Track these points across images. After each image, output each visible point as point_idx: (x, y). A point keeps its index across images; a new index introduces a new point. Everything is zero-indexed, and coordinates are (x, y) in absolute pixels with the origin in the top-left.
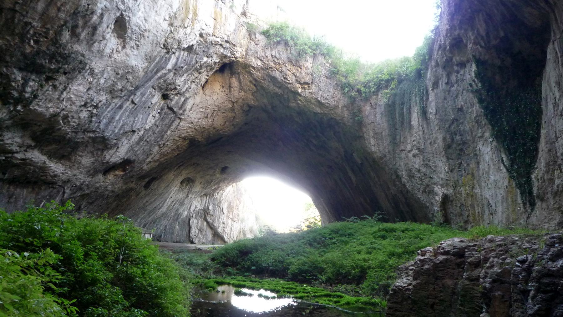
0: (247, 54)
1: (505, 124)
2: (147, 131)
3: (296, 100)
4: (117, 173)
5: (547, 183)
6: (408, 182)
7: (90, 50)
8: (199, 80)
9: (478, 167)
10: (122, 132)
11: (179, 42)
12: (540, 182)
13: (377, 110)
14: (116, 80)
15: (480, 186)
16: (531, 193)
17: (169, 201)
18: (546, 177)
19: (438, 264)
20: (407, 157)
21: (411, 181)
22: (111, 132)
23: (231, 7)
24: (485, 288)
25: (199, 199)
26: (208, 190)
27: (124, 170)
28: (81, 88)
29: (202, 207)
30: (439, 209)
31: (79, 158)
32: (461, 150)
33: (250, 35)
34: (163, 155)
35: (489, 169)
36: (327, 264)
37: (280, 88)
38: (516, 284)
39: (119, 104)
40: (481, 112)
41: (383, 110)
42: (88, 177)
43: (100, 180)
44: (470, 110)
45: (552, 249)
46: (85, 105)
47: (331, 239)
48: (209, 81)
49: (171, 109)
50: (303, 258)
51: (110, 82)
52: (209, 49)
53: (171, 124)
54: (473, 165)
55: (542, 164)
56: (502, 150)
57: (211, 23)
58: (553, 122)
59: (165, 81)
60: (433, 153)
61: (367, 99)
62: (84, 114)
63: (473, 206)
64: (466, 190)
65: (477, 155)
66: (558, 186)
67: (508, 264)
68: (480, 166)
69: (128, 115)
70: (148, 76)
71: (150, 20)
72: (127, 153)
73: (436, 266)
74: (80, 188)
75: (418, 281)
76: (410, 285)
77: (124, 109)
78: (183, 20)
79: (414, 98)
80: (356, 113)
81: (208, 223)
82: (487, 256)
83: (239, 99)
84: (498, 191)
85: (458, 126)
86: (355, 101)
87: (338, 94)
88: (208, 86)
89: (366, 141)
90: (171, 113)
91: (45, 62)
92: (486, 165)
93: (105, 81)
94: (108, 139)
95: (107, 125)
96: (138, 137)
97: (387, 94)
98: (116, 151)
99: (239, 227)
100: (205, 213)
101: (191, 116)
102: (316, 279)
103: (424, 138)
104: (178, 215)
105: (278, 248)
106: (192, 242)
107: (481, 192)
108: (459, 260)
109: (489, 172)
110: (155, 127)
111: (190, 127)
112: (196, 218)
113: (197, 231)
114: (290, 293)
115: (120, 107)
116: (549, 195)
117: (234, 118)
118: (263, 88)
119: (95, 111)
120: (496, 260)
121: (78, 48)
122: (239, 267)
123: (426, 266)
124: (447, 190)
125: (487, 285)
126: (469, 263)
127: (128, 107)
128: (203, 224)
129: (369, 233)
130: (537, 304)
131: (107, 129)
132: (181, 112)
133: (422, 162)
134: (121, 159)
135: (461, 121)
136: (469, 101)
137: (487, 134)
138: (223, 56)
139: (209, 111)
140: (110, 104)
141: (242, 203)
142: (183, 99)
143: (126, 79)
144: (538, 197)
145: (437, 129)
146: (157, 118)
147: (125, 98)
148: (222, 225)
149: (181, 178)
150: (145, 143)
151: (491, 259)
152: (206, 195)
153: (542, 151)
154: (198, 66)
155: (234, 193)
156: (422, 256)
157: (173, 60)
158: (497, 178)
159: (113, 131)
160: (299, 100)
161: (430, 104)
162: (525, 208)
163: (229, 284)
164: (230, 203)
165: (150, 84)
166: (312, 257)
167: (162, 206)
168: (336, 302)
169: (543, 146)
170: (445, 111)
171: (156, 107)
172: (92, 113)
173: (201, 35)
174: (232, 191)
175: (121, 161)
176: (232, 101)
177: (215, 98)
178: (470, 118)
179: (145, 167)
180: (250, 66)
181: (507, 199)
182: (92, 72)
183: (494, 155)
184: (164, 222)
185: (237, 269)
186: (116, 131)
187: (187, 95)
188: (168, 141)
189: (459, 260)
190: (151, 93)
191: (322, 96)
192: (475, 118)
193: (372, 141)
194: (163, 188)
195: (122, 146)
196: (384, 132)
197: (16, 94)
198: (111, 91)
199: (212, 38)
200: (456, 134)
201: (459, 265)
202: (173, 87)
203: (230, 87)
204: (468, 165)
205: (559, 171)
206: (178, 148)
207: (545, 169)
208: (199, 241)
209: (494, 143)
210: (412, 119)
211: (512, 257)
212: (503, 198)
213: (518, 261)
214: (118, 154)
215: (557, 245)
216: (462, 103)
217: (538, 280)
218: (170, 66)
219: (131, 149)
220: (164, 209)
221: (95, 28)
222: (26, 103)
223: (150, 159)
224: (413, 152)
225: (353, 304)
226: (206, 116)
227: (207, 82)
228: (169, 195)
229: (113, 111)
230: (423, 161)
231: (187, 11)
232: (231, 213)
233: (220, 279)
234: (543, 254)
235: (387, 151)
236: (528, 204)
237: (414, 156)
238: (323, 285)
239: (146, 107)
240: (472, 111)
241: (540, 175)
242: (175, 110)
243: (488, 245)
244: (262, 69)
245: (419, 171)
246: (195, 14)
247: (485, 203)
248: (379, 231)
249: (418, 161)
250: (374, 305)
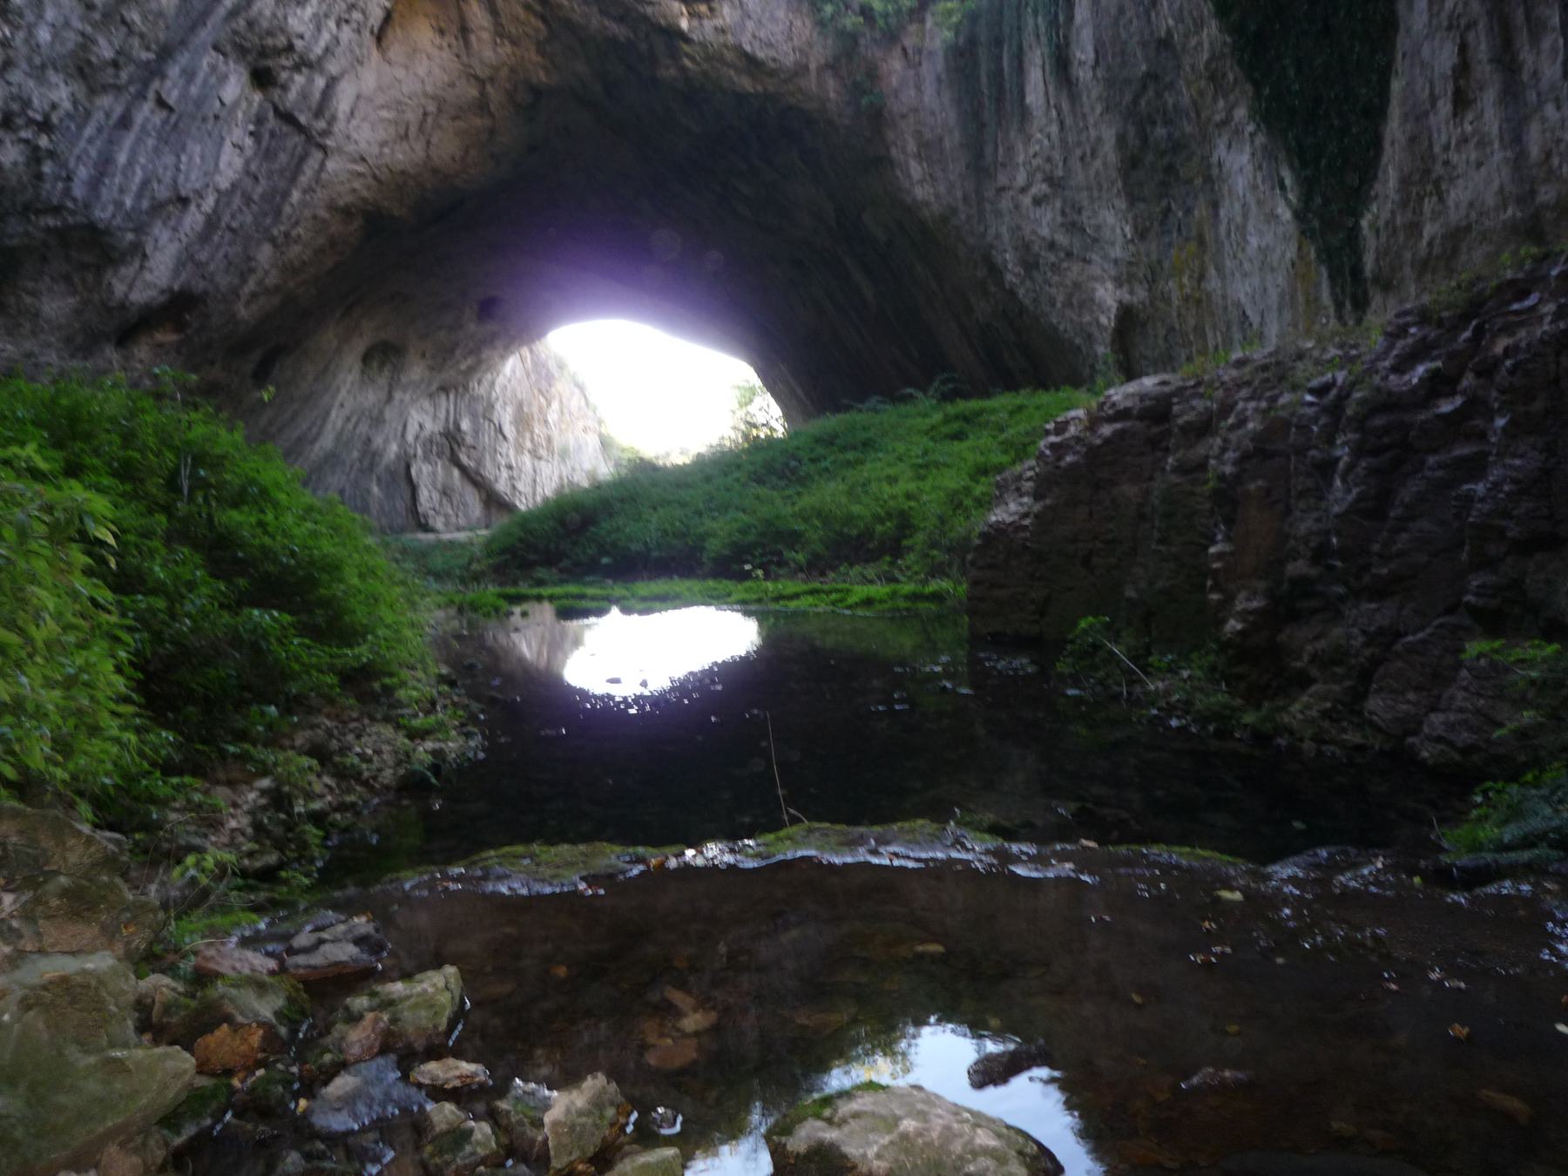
1: (1291, 72)
2: (224, 196)
3: (675, 55)
4: (160, 337)
5: (1401, 239)
6: (1022, 282)
8: (364, 13)
9: (1216, 215)
10: (145, 204)
12: (1383, 238)
13: (926, 68)
14: (89, 29)
15: (1220, 269)
16: (1357, 272)
17: (336, 418)
18: (1399, 221)
19: (1099, 447)
20: (1017, 207)
21: (1032, 280)
22: (111, 208)
24: (1222, 478)
25: (426, 404)
26: (449, 375)
27: (180, 327)
30: (1109, 350)
31: (28, 300)
32: (1170, 169)
34: (290, 270)
35: (1245, 216)
36: (806, 520)
37: (621, 19)
38: (1301, 451)
39: (118, 110)
40: (1225, 43)
41: (940, 64)
42: (73, 356)
43: (110, 362)
44: (1193, 42)
45: (1400, 343)
47: (813, 461)
48: (395, 16)
49: (287, 118)
50: (741, 515)
51: (72, 39)
54: (1201, 211)
55: (1391, 184)
56: (1282, 156)
58: (1426, 52)
59: (251, 24)
60: (1089, 189)
61: (891, 37)
63: (1200, 331)
64: (1182, 286)
65: (1212, 180)
66: (1430, 244)
67: (1283, 407)
68: (1222, 212)
69: (156, 150)
72: (176, 272)
73: (1093, 454)
75: (1048, 502)
76: (1025, 515)
77: (136, 128)
79: (1031, 21)
80: (863, 83)
81: (464, 470)
82: (1230, 401)
83: (496, 69)
84: (1269, 277)
85: (1159, 95)
86: (856, 43)
87: (804, 28)
89: (899, 173)
90: (292, 131)
92: (1237, 207)
93: (55, 35)
94: (107, 232)
95: (95, 184)
96: (200, 219)
97: (950, 13)
98: (142, 267)
99: (556, 473)
100: (450, 444)
101: (355, 135)
102: (781, 563)
103: (1063, 141)
104: (371, 456)
105: (669, 503)
106: (426, 528)
107: (1224, 287)
108: (1155, 430)
109: (1244, 226)
110: (248, 182)
111: (360, 175)
112: (426, 458)
113: (436, 496)
114: (711, 597)
115: (125, 122)
116: (1407, 270)
117: (492, 131)
118: (569, 25)
119: (44, 141)
120: (1252, 404)
122: (566, 563)
123: (1069, 459)
124: (1131, 292)
125: (1228, 469)
126: (1182, 428)
127: (147, 119)
128: (449, 474)
129: (919, 432)
130: (1356, 485)
131: (98, 197)
132: (321, 124)
133: (1059, 219)
134: (163, 292)
135: (1167, 79)
136: (1191, 13)
137: (1241, 113)
140: (88, 114)
141: (555, 405)
142: (320, 82)
143: (124, 22)
144: (1376, 280)
145: (1098, 110)
146: (249, 152)
147: (132, 89)
148: (505, 474)
149: (360, 346)
150: (228, 235)
151: (1241, 405)
152: (444, 389)
153: (1393, 143)
155: (528, 375)
156: (1057, 434)
158: (1269, 239)
159: (119, 205)
160: (687, 55)
161: (1078, 33)
162: (1340, 317)
163: (539, 598)
164: (520, 407)
165: (205, 35)
166: (765, 511)
167: (319, 434)
168: (833, 603)
169: (1395, 128)
170: (1123, 52)
171: (240, 115)
172: (37, 148)
174: (519, 373)
175: (162, 299)
176: (476, 77)
177: (421, 72)
178: (1193, 67)
181: (1293, 297)
183: (1259, 175)
185: (561, 571)
186: (128, 202)
187: (333, 68)
188: (297, 223)
189: (1155, 430)
190: (213, 68)
191: (754, 36)
192: (1208, 63)
193: (916, 170)
194: (310, 377)
195: (156, 248)
196: (947, 139)
198: (82, 69)
200: (1154, 123)
201: (1155, 443)
202: (281, 41)
203: (464, 31)
204: (1188, 211)
205: (1435, 198)
206: (333, 242)
207: (1397, 198)
208: (447, 524)
209: (1261, 139)
210: (1029, 89)
211: (1295, 388)
212: (1281, 296)
213: (1312, 391)
214: (148, 276)
215: (1413, 330)
216: (1171, 22)
217: (1360, 423)
219: (187, 259)
220: (327, 441)
223: (251, 285)
224: (1034, 190)
225: (881, 601)
226: (402, 131)
228: (334, 397)
229: (105, 135)
230: (1063, 213)
232: (528, 435)
233: (511, 590)
234: (1378, 359)
235: (959, 194)
236: (1348, 306)
237: (1037, 202)
238: (800, 575)
240: (1200, 44)
241: (1385, 215)
242: (303, 119)
243: (1234, 373)
245: (1052, 246)
247: (1234, 314)
248: (947, 420)
249: (1049, 215)
250: (937, 597)
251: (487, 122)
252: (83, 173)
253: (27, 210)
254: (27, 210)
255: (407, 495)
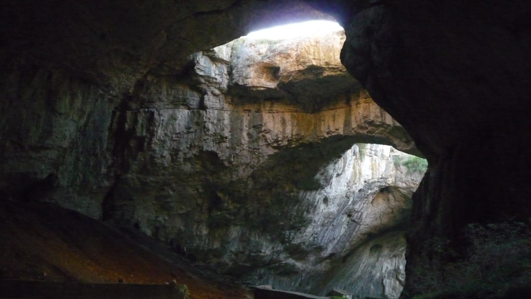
0: (395, 181)
2: (341, 237)
7: (314, 214)
11: (354, 193)
17: (362, 266)
23: (382, 155)
25: (389, 261)
27: (331, 259)
28: (310, 229)
29: (393, 268)
33: (396, 167)
46: (312, 235)
49: (354, 221)
52: (371, 186)
53: (355, 229)
57: (370, 172)
62: (311, 239)
70: (339, 212)
71: (338, 190)
72: (332, 250)
74: (309, 273)
78: (354, 181)
88: (375, 201)
91: (297, 225)
104: (371, 277)
112: (388, 278)
113: (391, 290)
115: (327, 230)
117: (395, 217)
121: (309, 216)
128: (395, 283)
138: (380, 186)
139: (377, 216)
142: (360, 214)
152: (395, 256)
154: (366, 196)
157: (351, 199)
173: (365, 182)
177: (380, 207)
179: (343, 254)
180: (399, 187)
182: (315, 222)
184: (361, 284)
187: (362, 211)
197: (287, 240)
199: (371, 181)
203: (388, 200)
206: (361, 240)
218: (350, 203)
219: (334, 247)
220: (359, 273)
221: (316, 207)
222: (289, 242)
223: (344, 250)
227: (373, 199)
231: (356, 175)
239: (339, 225)
244: (407, 188)
246: (360, 174)
251: (393, 215)
252: (320, 238)
253: (312, 245)
254: (312, 245)
255: (382, 289)
